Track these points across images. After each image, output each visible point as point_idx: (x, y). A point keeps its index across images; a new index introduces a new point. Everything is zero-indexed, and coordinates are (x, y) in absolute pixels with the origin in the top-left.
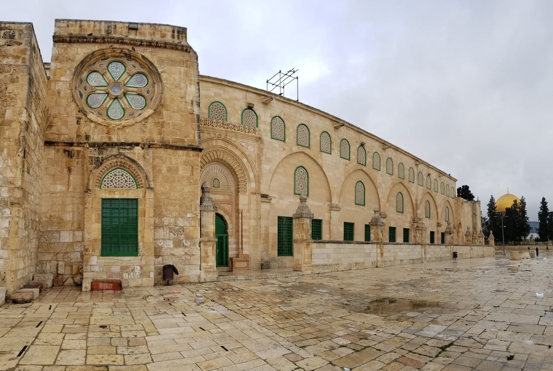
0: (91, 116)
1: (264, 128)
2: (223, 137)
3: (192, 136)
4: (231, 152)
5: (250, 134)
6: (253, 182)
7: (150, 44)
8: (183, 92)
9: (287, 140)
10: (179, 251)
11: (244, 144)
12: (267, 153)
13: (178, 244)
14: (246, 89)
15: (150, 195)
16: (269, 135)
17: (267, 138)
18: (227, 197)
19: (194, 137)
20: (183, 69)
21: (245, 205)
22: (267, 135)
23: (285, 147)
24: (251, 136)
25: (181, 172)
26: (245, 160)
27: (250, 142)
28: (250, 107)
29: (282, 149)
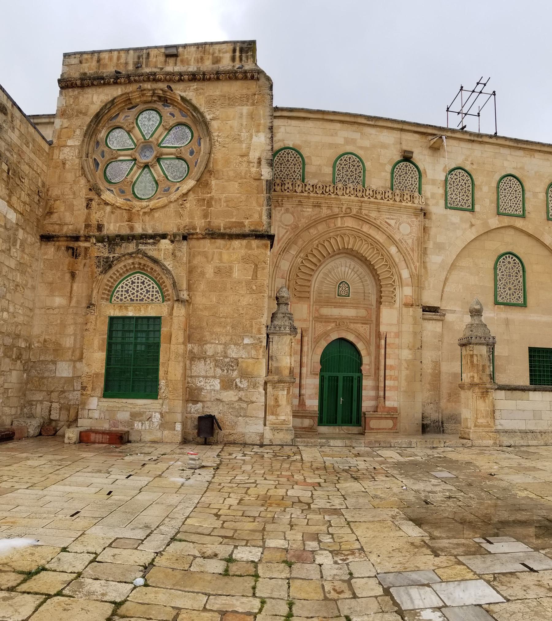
0: (107, 196)
1: (433, 191)
2: (354, 211)
3: (256, 216)
4: (369, 236)
5: (404, 204)
6: (407, 285)
7: (194, 77)
8: (244, 146)
9: (477, 208)
10: (230, 396)
11: (392, 222)
12: (438, 235)
13: (228, 384)
14: (400, 126)
15: (180, 311)
16: (442, 202)
17: (437, 209)
18: (362, 313)
19: (261, 217)
20: (245, 110)
21: (391, 325)
22: (437, 204)
23: (473, 221)
24: (406, 207)
25: (236, 274)
27: (404, 218)
29: (468, 225)
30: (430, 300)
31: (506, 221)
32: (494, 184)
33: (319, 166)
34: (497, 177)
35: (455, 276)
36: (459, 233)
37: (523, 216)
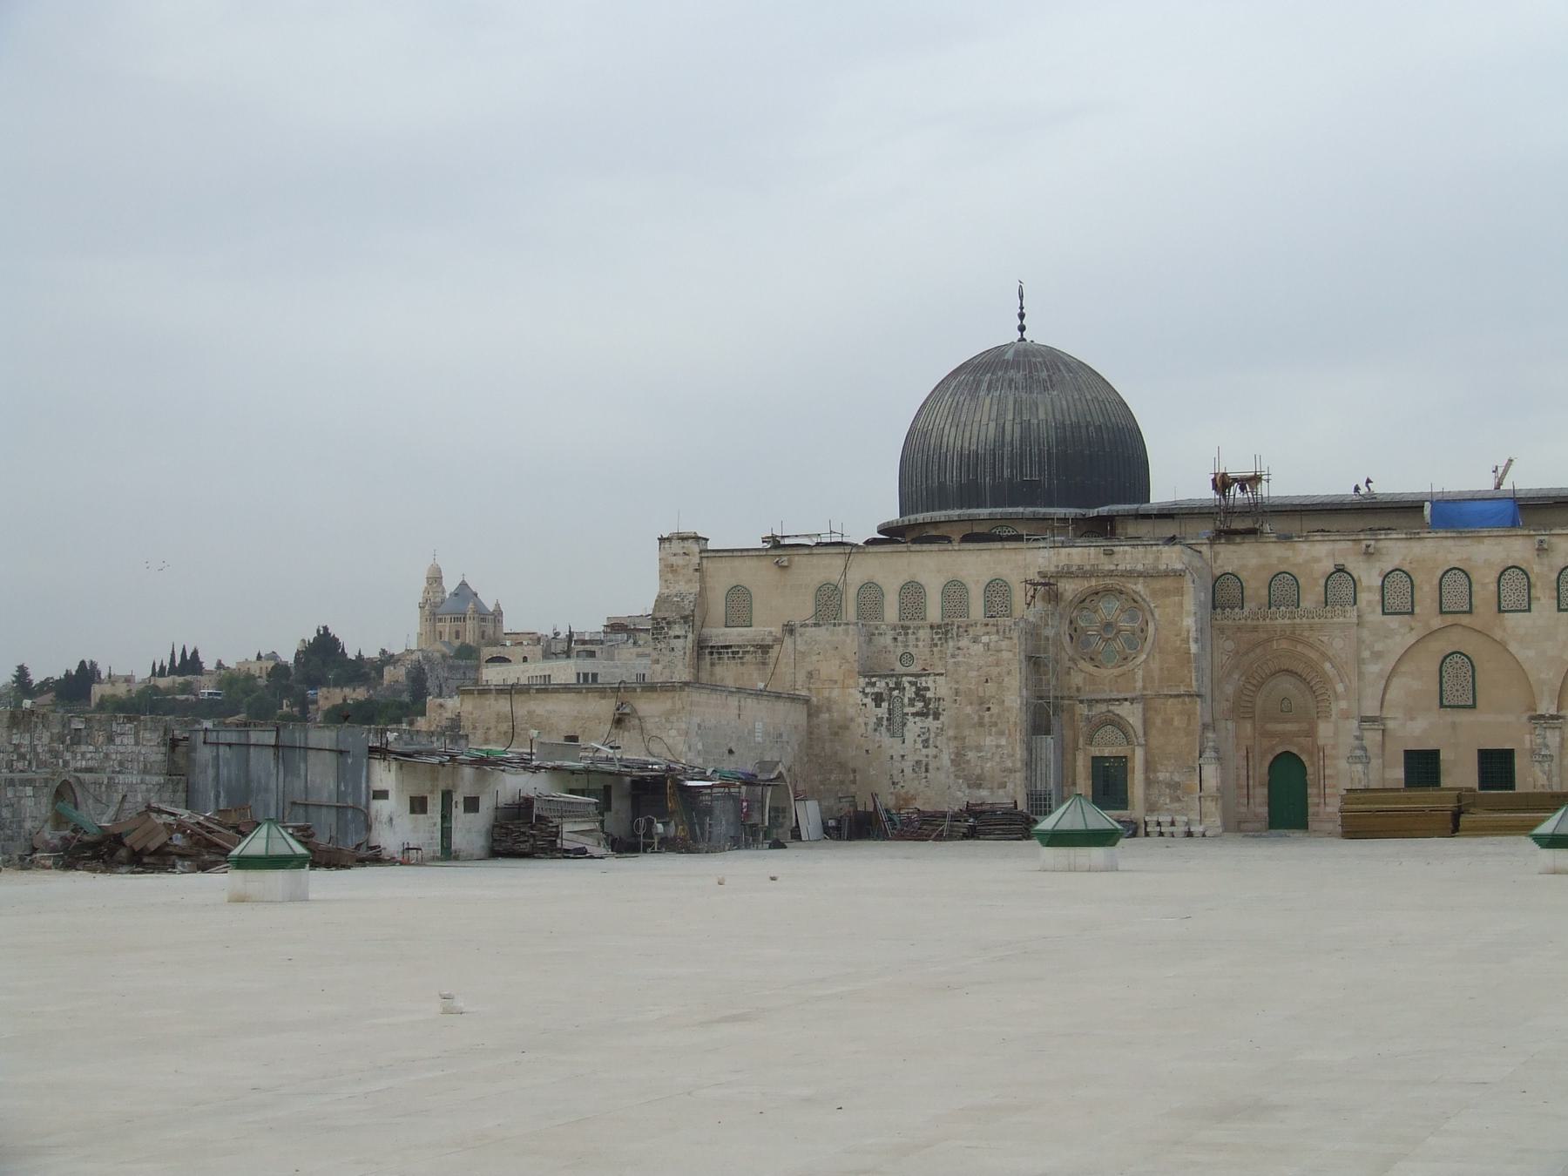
1: (1369, 597)
9: (1417, 610)
11: (1325, 639)
16: (1379, 609)
18: (1305, 726)
22: (1373, 611)
26: (1327, 666)
28: (1340, 569)
30: (1370, 709)
31: (1450, 619)
32: (1436, 581)
33: (1256, 588)
34: (1440, 573)
35: (1395, 682)
36: (1398, 639)
37: (1470, 612)
